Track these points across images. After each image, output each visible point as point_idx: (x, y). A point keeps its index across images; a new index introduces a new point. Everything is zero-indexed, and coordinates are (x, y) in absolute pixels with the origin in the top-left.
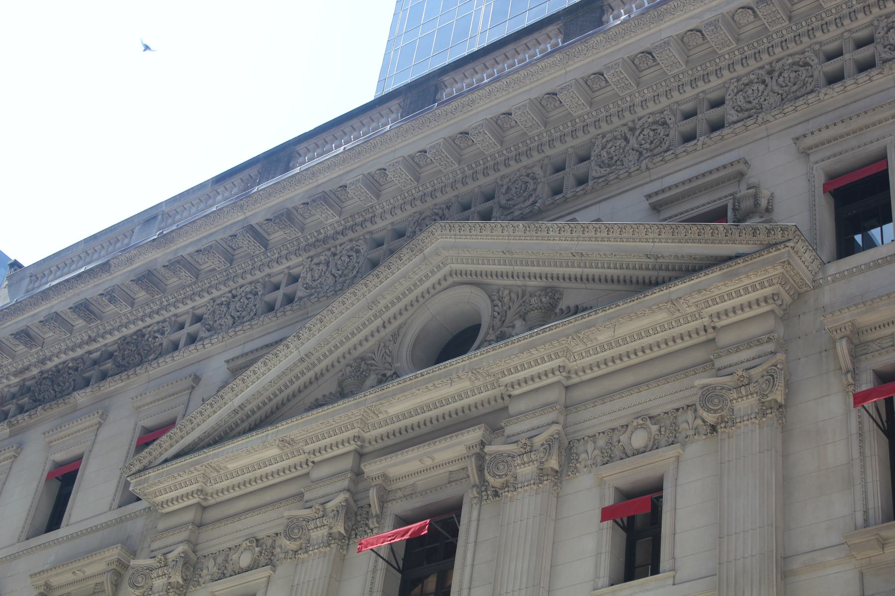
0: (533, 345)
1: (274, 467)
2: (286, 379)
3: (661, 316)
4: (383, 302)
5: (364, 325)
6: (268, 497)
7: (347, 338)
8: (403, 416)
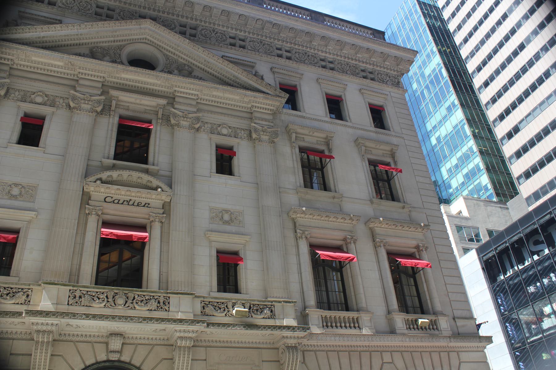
0: (194, 84)
1: (56, 69)
2: (67, 37)
3: (237, 97)
4: (118, 33)
5: (107, 37)
6: (51, 79)
7: (98, 38)
8: (127, 80)
